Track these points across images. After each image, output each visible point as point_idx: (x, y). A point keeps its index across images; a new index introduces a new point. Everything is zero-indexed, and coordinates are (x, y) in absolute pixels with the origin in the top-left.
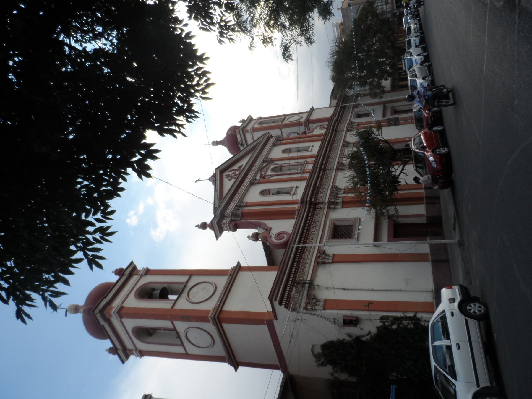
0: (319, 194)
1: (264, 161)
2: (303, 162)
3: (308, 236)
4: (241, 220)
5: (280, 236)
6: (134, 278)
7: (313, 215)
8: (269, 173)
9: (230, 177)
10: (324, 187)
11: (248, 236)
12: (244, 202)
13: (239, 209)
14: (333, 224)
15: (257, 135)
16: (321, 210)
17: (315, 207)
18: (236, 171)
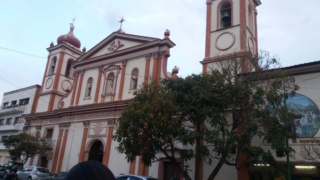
5: (62, 104)
8: (108, 73)
18: (117, 46)
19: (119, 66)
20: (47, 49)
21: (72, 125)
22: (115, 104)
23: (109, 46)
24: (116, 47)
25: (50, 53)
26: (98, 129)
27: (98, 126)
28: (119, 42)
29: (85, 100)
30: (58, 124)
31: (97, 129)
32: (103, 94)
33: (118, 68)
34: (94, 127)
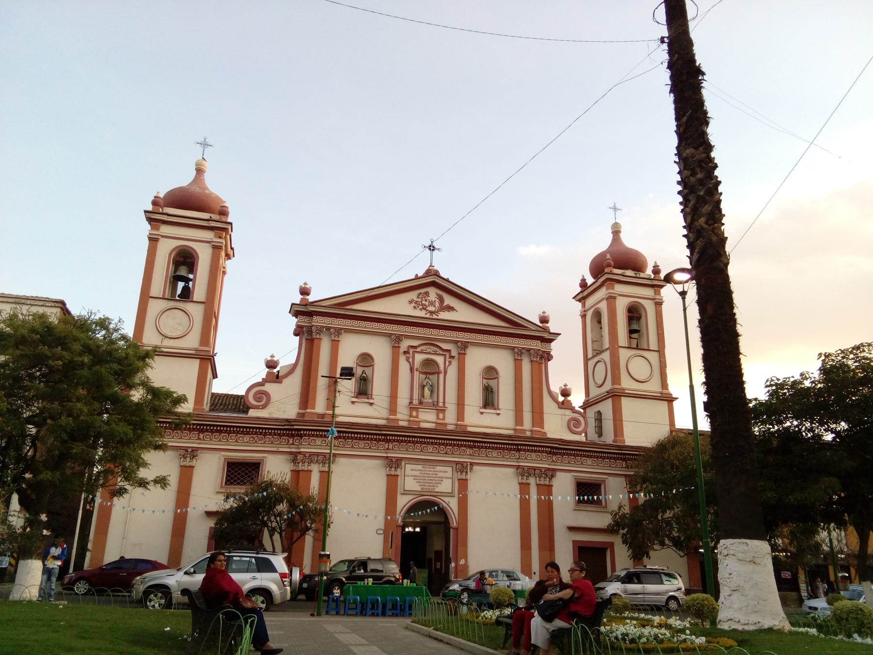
0: (323, 439)
1: (456, 342)
2: (444, 403)
3: (234, 432)
4: (306, 339)
6: (209, 235)
7: (279, 435)
9: (420, 300)
10: (341, 443)
11: (275, 355)
12: (338, 337)
13: (321, 334)
14: (259, 461)
15: (603, 306)
16: (291, 444)
17: (296, 436)
18: (437, 304)
19: (449, 351)
20: (146, 212)
21: (341, 461)
22: (483, 436)
23: (413, 295)
24: (435, 306)
25: (153, 228)
26: (428, 480)
27: (429, 474)
28: (441, 300)
29: (356, 403)
30: (291, 453)
31: (427, 478)
32: (414, 403)
33: (447, 354)
34: (417, 473)
